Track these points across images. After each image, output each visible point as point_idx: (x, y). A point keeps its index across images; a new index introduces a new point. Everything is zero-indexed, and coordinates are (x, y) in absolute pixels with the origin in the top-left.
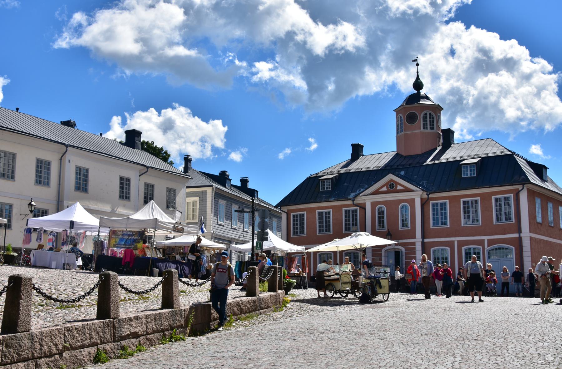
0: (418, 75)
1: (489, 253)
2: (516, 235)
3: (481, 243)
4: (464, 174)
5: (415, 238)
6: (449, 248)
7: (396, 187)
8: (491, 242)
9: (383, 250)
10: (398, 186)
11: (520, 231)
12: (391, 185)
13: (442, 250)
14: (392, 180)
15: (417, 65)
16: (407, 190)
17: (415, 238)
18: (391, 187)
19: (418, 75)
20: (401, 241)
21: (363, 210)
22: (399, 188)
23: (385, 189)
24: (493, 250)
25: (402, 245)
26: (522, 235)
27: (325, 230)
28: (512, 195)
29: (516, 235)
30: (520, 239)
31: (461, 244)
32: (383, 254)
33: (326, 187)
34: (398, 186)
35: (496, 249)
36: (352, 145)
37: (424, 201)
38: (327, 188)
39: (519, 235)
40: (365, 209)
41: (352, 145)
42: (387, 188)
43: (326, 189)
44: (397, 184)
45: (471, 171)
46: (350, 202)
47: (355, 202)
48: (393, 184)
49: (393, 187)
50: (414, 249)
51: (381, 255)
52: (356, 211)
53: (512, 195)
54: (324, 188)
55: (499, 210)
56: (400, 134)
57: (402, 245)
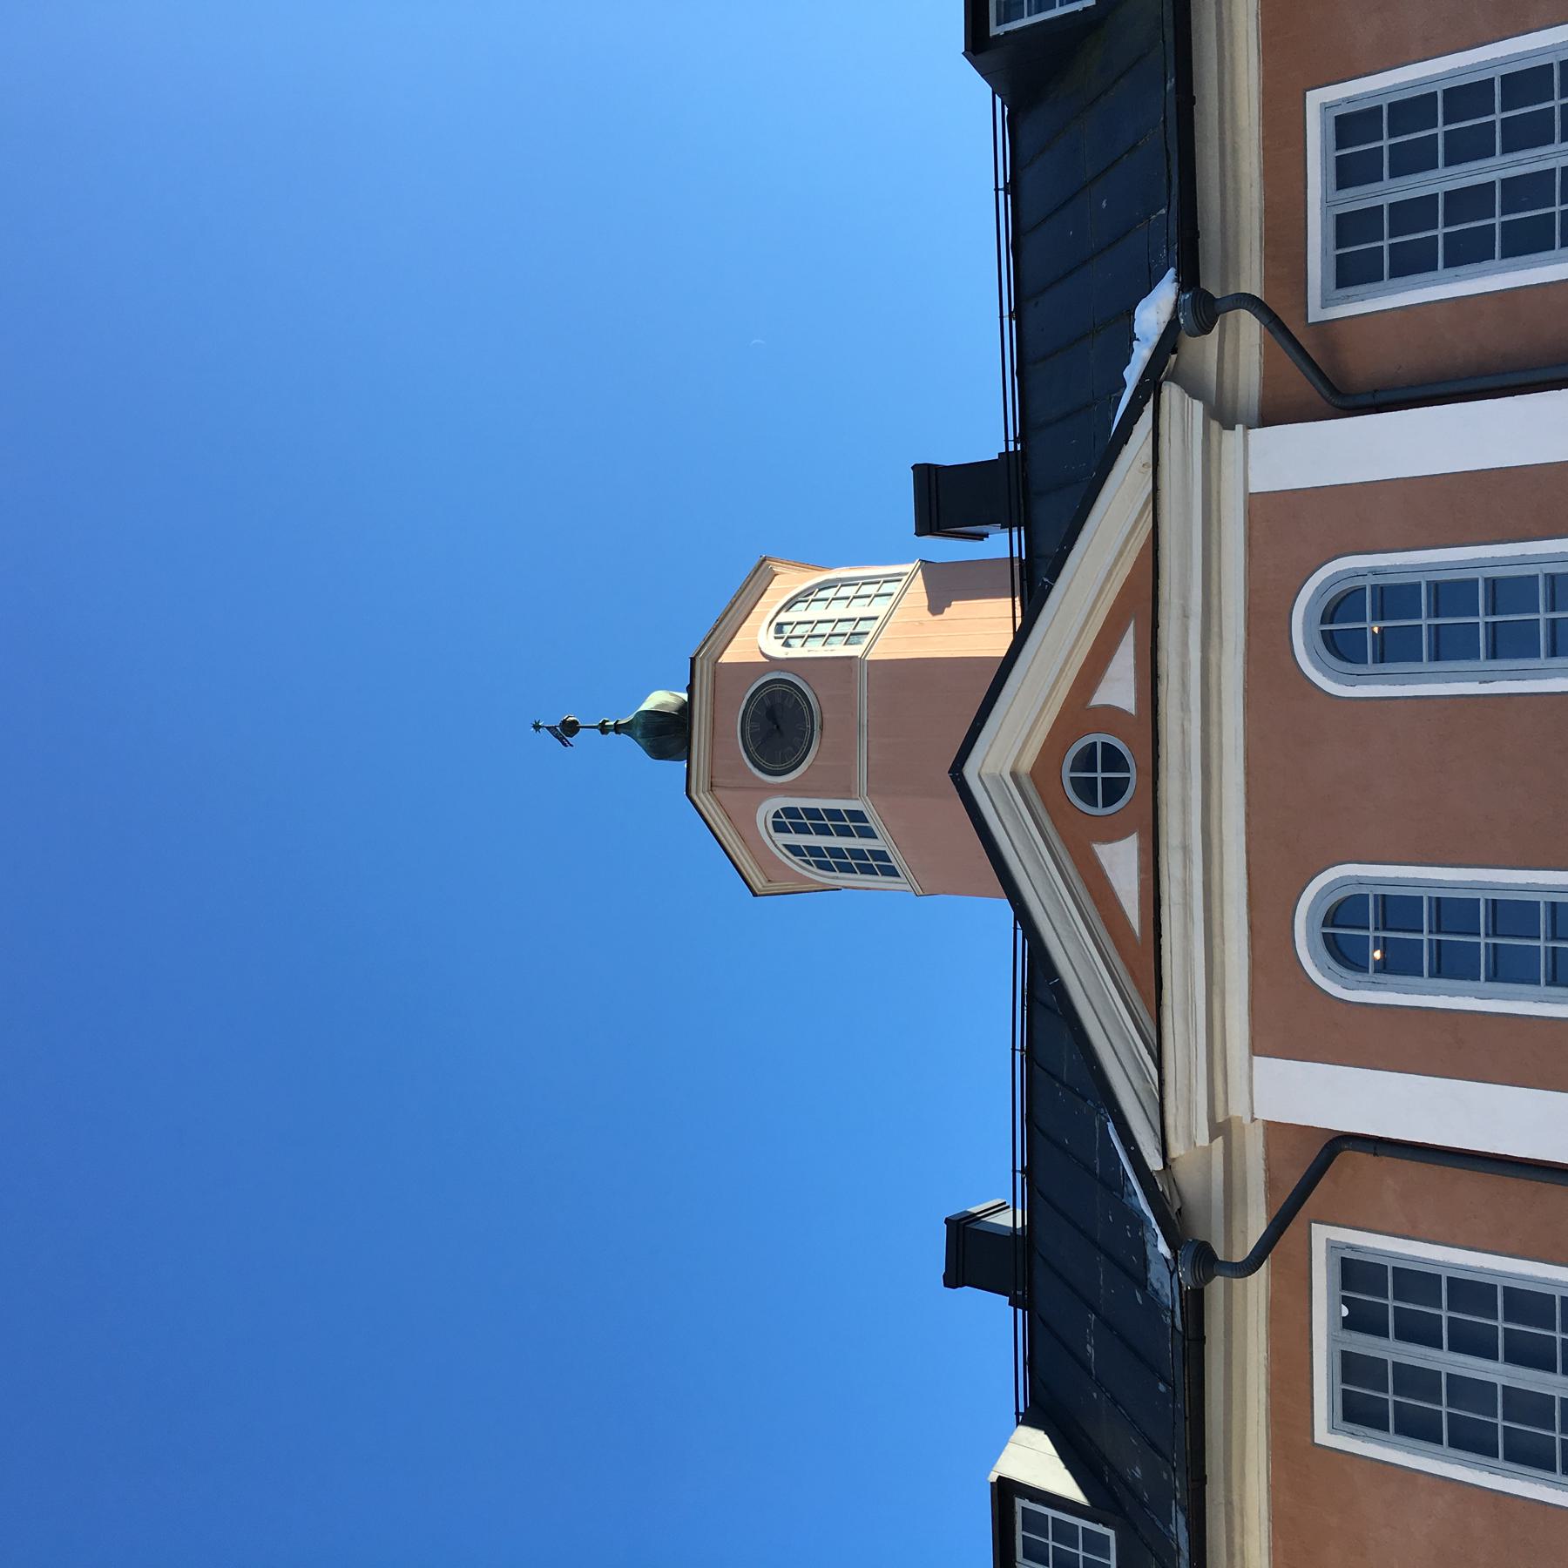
0: (617, 728)
10: (1099, 699)
12: (1086, 789)
14: (1039, 780)
19: (617, 728)
21: (1348, 1158)
22: (1119, 689)
23: (1120, 860)
34: (1099, 699)
36: (953, 1279)
37: (1301, 386)
40: (1340, 1143)
41: (953, 1279)
48: (1086, 759)
49: (1113, 759)
52: (1355, 1274)
56: (897, 860)
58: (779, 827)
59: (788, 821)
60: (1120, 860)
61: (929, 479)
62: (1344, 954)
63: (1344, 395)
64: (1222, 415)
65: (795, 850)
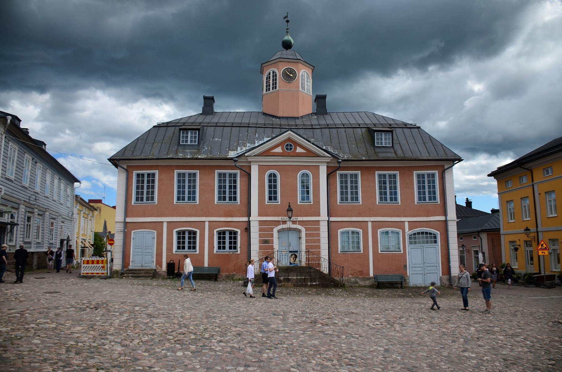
1: (410, 238)
2: (442, 218)
3: (400, 225)
4: (378, 143)
5: (319, 215)
6: (361, 231)
7: (296, 149)
8: (412, 225)
9: (275, 230)
11: (445, 214)
12: (287, 145)
13: (353, 232)
15: (288, 21)
16: (310, 154)
17: (319, 215)
18: (287, 149)
20: (300, 219)
22: (299, 150)
23: (279, 150)
24: (415, 234)
25: (302, 223)
26: (448, 219)
27: (186, 198)
28: (437, 172)
29: (442, 218)
30: (446, 222)
31: (376, 225)
32: (275, 234)
33: (189, 139)
35: (418, 233)
36: (205, 98)
38: (191, 141)
39: (446, 218)
40: (249, 175)
42: (282, 149)
43: (189, 143)
44: (297, 144)
45: (386, 139)
46: (233, 164)
47: (238, 164)
48: (291, 145)
49: (291, 149)
50: (318, 229)
51: (272, 235)
53: (437, 172)
54: (187, 141)
55: (421, 188)
57: (302, 223)
58: (273, 72)
59: (275, 75)
60: (279, 150)
61: (324, 97)
62: (270, 176)
63: (330, 175)
64: (328, 163)
65: (269, 74)
